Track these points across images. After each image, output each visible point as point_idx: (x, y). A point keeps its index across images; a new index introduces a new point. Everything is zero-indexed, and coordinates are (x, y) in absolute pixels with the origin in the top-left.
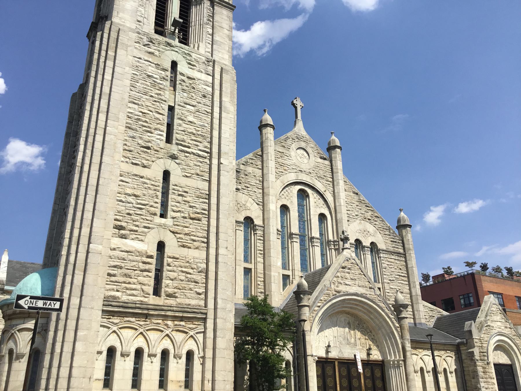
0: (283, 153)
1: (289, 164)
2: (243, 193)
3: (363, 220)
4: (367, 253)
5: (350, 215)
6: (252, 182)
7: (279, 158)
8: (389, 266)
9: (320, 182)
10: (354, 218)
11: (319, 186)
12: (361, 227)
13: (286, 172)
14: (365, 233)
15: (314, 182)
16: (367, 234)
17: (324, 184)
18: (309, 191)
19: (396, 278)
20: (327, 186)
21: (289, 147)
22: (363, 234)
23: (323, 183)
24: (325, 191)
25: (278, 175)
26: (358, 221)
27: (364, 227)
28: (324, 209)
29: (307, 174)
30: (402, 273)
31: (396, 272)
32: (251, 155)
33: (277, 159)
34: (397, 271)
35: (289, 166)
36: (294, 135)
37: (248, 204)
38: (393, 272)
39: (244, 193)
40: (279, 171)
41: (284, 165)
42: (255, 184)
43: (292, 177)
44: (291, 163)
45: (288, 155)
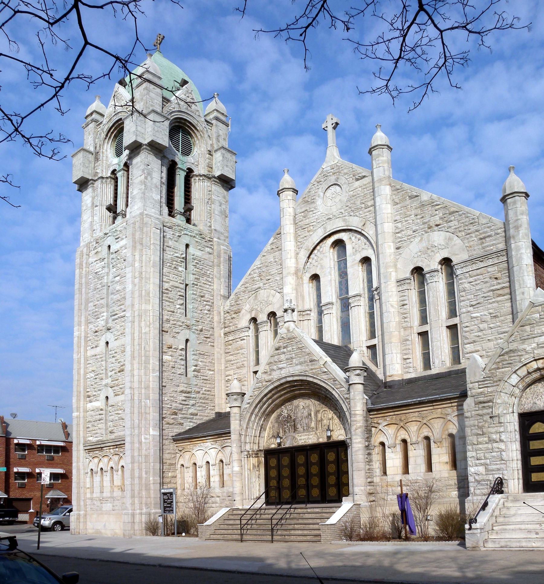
0: (306, 210)
1: (312, 221)
2: (265, 289)
3: (426, 232)
4: (431, 281)
5: (403, 238)
6: (273, 271)
7: (302, 220)
8: (472, 283)
9: (357, 216)
10: (409, 239)
11: (355, 223)
12: (424, 244)
13: (311, 233)
14: (429, 251)
15: (349, 222)
16: (432, 251)
17: (362, 216)
18: (343, 236)
19: (485, 297)
20: (367, 215)
21: (313, 198)
22: (426, 255)
23: (360, 214)
24: (364, 225)
25: (299, 244)
26: (417, 240)
27: (429, 241)
28: (366, 251)
29: (338, 216)
30: (499, 283)
31: (486, 287)
32: (272, 239)
33: (300, 223)
34: (488, 285)
35: (314, 222)
36: (320, 176)
37: (271, 298)
38: (479, 290)
39: (265, 288)
40: (302, 238)
41: (308, 226)
42: (277, 271)
43: (320, 234)
44: (316, 217)
45: (312, 209)
